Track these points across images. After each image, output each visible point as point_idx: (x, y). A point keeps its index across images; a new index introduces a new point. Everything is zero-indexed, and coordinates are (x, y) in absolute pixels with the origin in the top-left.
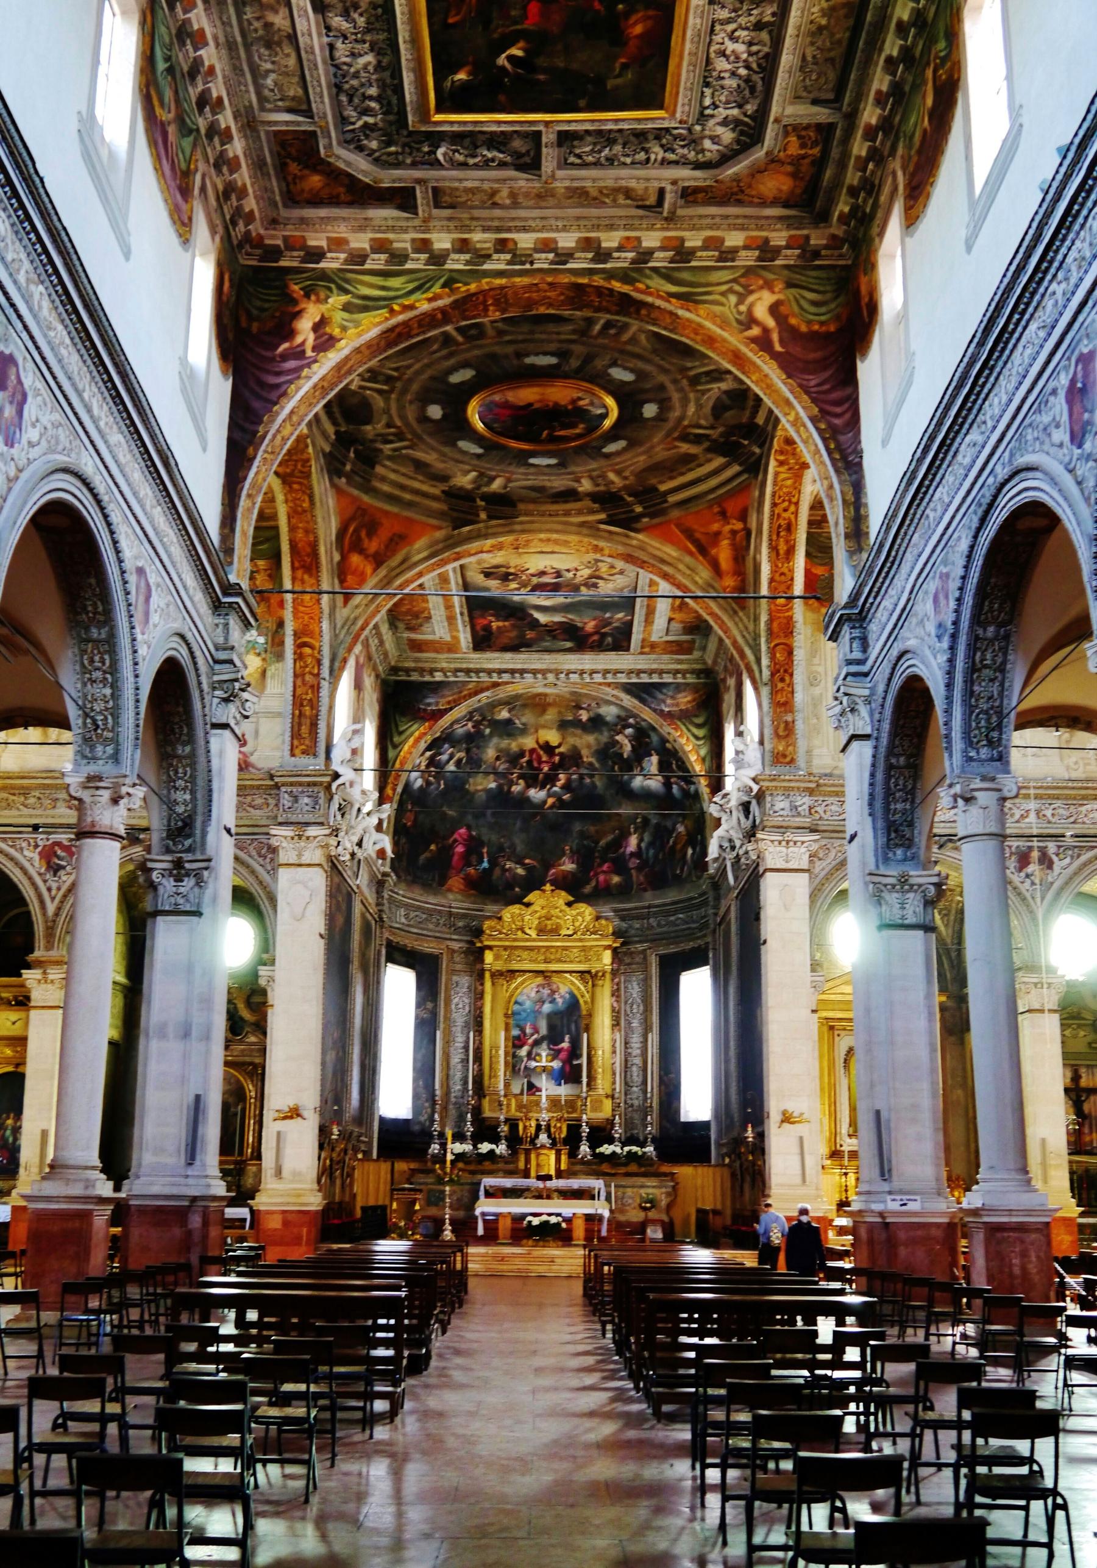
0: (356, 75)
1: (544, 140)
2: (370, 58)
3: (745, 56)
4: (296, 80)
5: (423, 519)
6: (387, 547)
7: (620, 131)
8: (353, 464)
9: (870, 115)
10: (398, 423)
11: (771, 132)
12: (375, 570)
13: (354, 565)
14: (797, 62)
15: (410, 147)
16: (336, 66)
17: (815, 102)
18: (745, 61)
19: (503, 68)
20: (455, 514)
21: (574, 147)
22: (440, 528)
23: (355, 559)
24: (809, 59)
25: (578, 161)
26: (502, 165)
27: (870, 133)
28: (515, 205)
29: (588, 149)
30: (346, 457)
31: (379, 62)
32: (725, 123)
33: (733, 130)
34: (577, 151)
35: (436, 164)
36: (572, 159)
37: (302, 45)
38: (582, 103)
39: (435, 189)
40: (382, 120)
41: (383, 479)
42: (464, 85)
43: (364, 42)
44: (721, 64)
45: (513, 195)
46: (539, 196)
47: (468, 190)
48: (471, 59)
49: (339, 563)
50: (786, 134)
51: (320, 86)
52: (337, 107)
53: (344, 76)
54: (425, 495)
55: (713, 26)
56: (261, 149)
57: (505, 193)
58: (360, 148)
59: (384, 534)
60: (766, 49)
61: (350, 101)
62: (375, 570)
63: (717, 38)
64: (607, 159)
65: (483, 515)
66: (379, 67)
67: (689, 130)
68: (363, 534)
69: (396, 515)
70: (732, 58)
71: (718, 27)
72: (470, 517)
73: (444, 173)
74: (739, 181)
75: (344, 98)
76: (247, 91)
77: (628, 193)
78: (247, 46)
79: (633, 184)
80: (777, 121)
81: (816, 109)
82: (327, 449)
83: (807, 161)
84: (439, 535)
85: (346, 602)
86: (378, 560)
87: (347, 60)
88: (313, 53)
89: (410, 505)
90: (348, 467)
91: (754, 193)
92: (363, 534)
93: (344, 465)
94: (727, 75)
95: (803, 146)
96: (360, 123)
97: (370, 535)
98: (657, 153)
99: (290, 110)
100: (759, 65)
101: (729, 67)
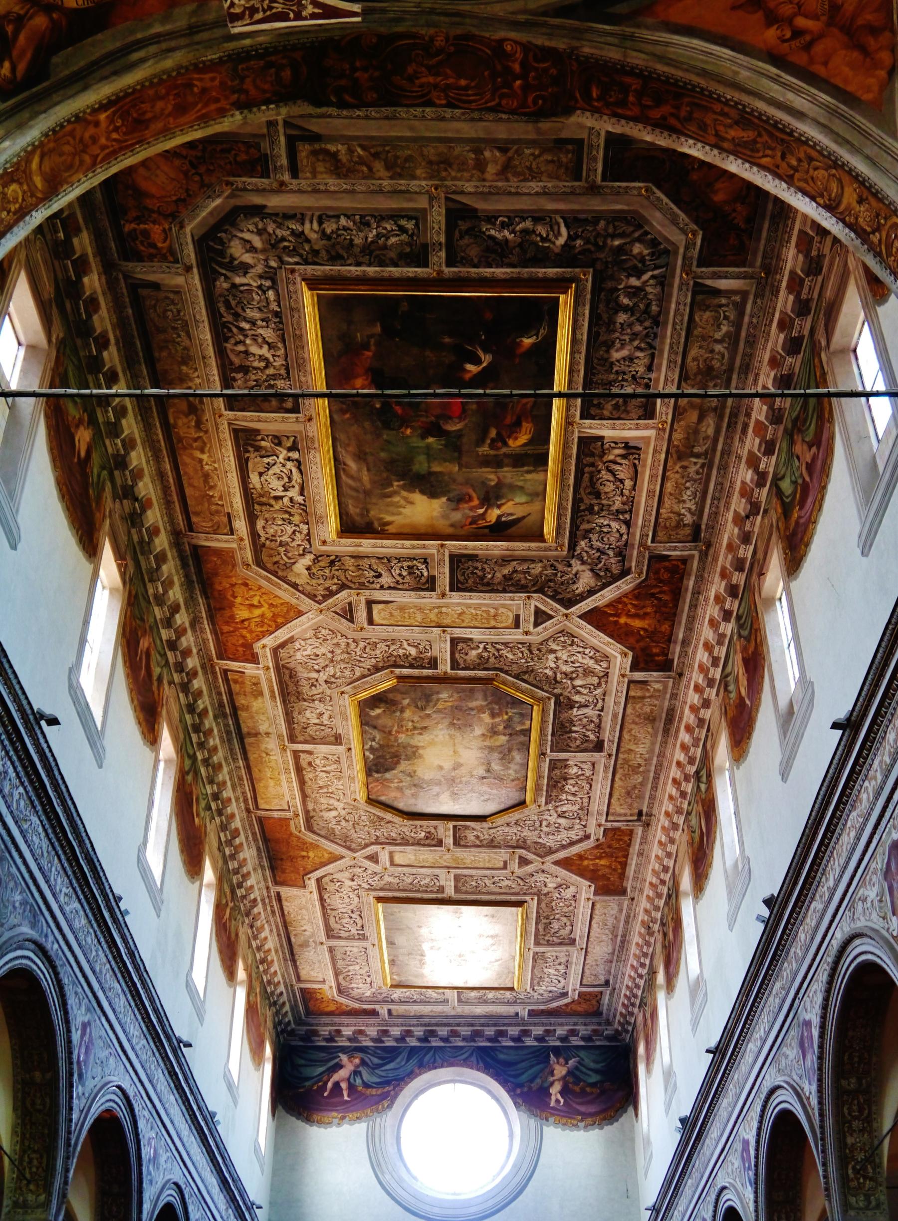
0: (635, 336)
1: (443, 254)
2: (616, 355)
3: (248, 341)
4: (697, 331)
7: (359, 264)
9: (93, 282)
11: (190, 253)
14: (194, 332)
15: (596, 244)
16: (652, 347)
17: (156, 286)
18: (246, 336)
19: (485, 351)
21: (409, 244)
24: (182, 334)
25: (403, 222)
26: (491, 219)
27: (82, 267)
28: (477, 145)
29: (393, 240)
31: (608, 351)
32: (245, 268)
33: (233, 259)
34: (404, 237)
35: (573, 220)
36: (410, 225)
37: (678, 370)
38: (405, 306)
39: (578, 178)
40: (619, 281)
42: (526, 333)
43: (617, 373)
44: (268, 333)
45: (481, 166)
46: (445, 162)
47: (534, 175)
48: (517, 361)
50: (171, 251)
51: (674, 323)
52: (663, 299)
53: (647, 335)
55: (288, 373)
56: (768, 240)
57: (491, 169)
58: (654, 243)
60: (229, 346)
61: (648, 305)
63: (279, 362)
64: (368, 225)
66: (609, 345)
67: (282, 262)
70: (260, 340)
71: (283, 372)
73: (562, 206)
74: (203, 185)
75: (654, 308)
76: (752, 316)
77: (338, 169)
78: (730, 370)
79: (333, 183)
80: (188, 269)
81: (152, 278)
83: (133, 214)
87: (639, 354)
88: (669, 361)
91: (177, 162)
94: (259, 323)
95: (146, 234)
96: (645, 277)
98: (310, 229)
99: (717, 292)
100: (230, 330)
101: (260, 331)
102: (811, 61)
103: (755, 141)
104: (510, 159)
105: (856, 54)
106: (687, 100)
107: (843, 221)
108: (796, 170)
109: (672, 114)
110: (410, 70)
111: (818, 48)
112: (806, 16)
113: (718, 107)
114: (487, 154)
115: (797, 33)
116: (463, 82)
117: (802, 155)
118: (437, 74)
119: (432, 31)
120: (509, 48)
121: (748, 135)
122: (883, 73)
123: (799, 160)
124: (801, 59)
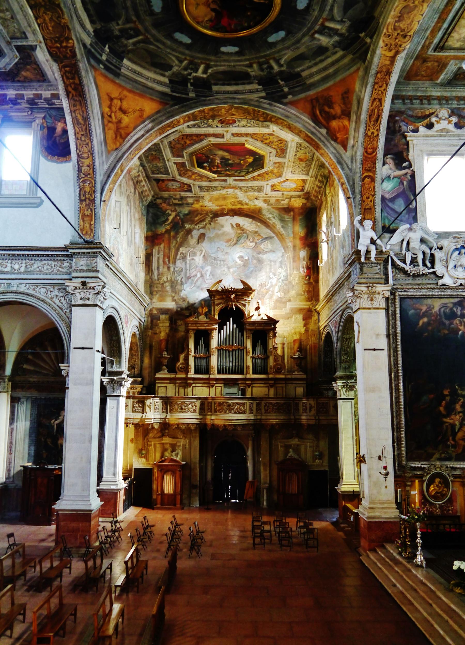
5: (348, 73)
6: (344, 104)
8: (287, 86)
10: (248, 63)
12: (349, 120)
13: (337, 128)
20: (357, 55)
22: (358, 69)
23: (334, 124)
30: (281, 87)
41: (311, 75)
49: (327, 133)
54: (337, 61)
59: (337, 98)
62: (349, 120)
65: (368, 40)
68: (327, 109)
69: (334, 85)
72: (364, 48)
82: (263, 94)
84: (361, 73)
85: (345, 147)
86: (347, 114)
89: (335, 73)
90: (286, 89)
92: (327, 109)
93: (283, 90)
97: (331, 107)
102: (107, 125)
103: (81, 124)
104: (9, 20)
105: (114, 136)
106: (80, 99)
107: (78, 162)
108: (81, 140)
109: (73, 95)
110: (48, 13)
111: (110, 125)
112: (115, 115)
113: (84, 109)
114: (8, 13)
115: (110, 116)
116: (51, 28)
117: (87, 141)
118: (50, 20)
119: (67, 18)
120: (71, 41)
121: (81, 120)
122: (115, 147)
123: (85, 141)
124: (106, 122)
